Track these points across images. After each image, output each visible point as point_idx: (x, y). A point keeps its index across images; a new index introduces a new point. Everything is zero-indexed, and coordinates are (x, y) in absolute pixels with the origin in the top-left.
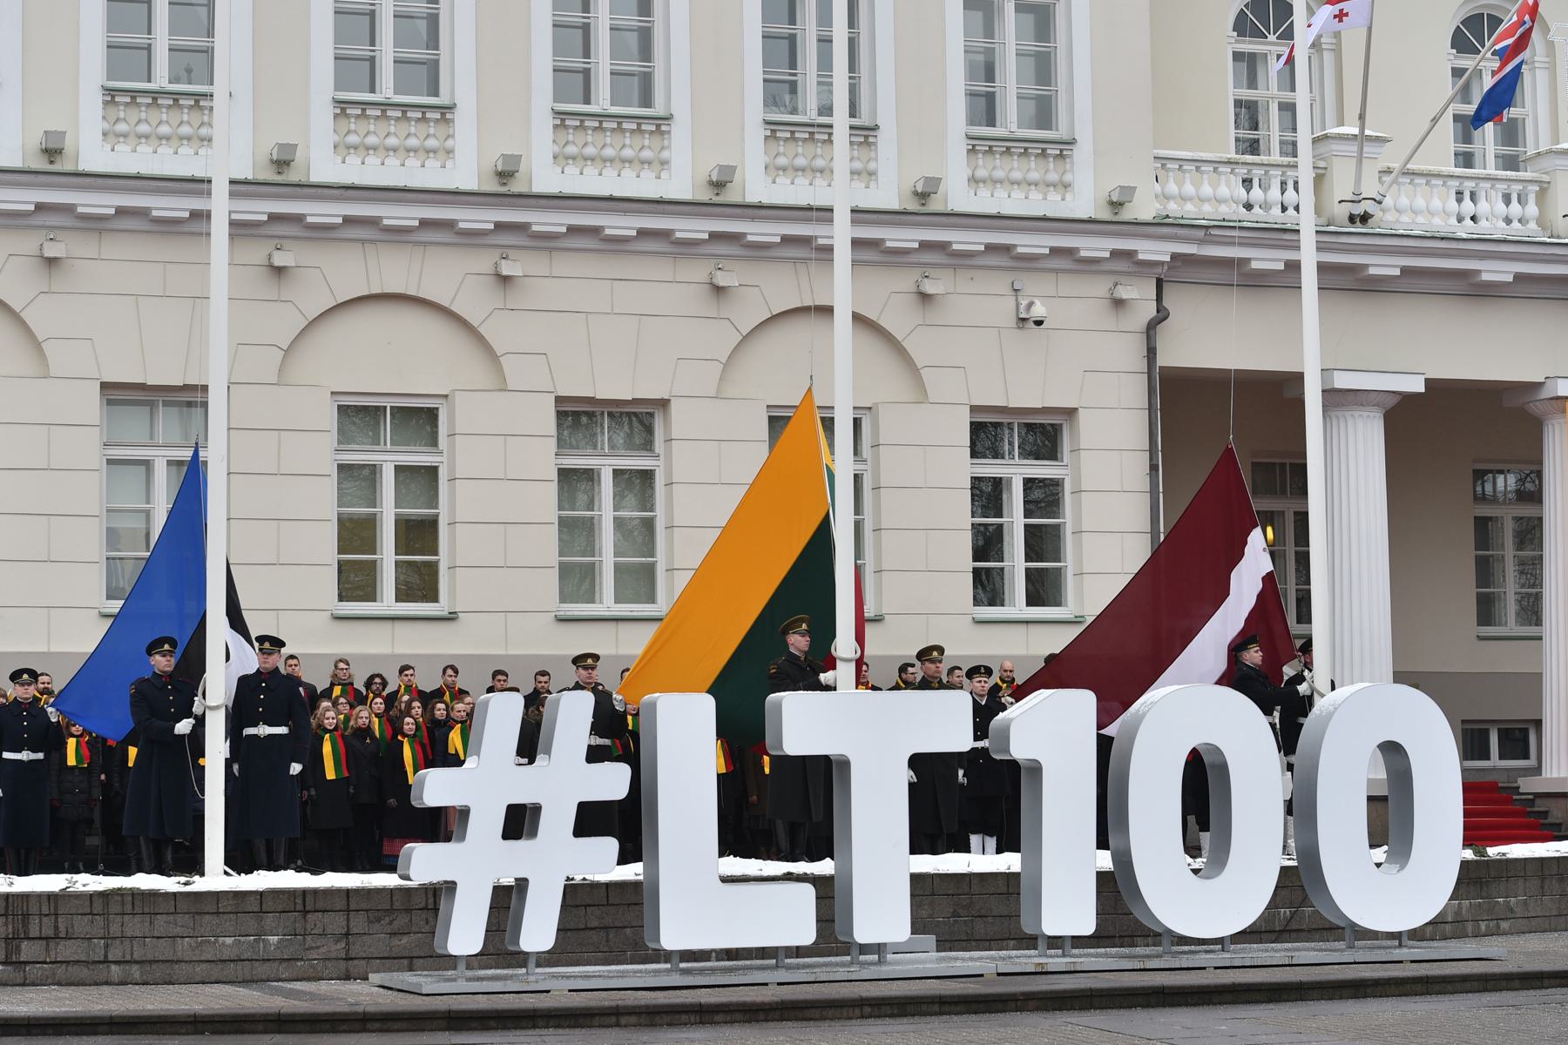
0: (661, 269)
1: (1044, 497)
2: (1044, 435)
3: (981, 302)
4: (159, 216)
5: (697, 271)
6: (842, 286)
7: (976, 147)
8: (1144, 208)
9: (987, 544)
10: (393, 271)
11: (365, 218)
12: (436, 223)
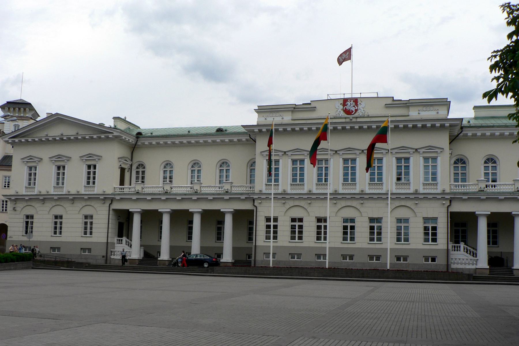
0: (382, 201)
1: (434, 229)
4: (321, 198)
7: (424, 184)
8: (448, 191)
11: (344, 197)
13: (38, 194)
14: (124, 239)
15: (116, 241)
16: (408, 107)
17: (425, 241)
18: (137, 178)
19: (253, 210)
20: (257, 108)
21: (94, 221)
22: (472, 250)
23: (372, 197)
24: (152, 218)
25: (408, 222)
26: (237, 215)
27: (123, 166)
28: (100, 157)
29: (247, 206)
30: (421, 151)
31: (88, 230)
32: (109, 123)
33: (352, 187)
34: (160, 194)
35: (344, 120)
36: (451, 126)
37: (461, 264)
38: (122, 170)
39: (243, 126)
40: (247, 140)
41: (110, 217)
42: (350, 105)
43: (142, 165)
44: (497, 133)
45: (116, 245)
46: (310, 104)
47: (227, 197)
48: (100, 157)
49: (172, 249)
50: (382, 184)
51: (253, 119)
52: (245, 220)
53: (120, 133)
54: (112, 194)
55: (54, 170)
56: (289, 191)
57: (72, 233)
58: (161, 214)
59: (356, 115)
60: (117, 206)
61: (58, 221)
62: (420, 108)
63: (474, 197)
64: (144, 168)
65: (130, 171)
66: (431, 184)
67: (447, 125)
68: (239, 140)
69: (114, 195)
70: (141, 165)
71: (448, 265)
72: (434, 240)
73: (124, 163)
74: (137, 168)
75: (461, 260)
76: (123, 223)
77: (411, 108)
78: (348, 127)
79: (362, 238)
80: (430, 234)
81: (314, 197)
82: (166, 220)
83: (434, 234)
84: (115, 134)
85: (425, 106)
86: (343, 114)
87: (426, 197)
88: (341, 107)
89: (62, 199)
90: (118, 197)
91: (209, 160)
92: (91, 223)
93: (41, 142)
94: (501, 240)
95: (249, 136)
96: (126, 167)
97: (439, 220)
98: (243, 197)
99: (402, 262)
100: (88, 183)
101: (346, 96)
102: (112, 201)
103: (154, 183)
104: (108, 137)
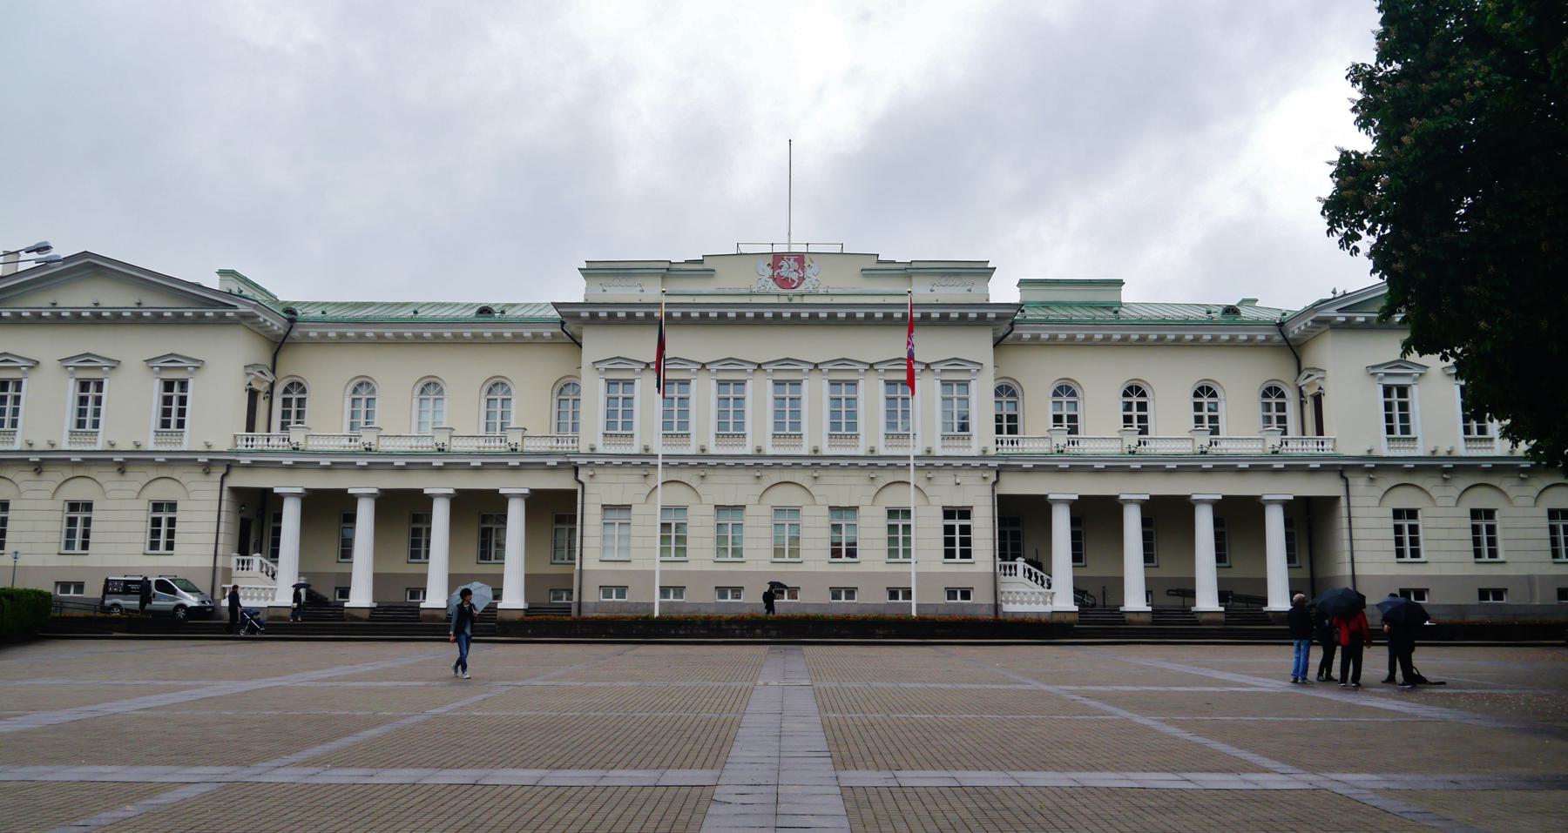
0: (857, 473)
1: (966, 530)
2: (965, 513)
3: (945, 480)
5: (866, 473)
6: (912, 477)
7: (944, 437)
9: (949, 542)
10: (787, 476)
11: (778, 462)
12: (796, 463)
13: (26, 448)
14: (256, 559)
15: (234, 565)
16: (909, 276)
17: (947, 556)
18: (286, 414)
19: (575, 492)
20: (584, 266)
21: (179, 516)
22: (1040, 573)
23: (837, 464)
24: (330, 511)
25: (968, 517)
26: (538, 503)
27: (255, 386)
28: (199, 365)
29: (562, 482)
30: (938, 368)
31: (163, 539)
32: (214, 282)
33: (792, 441)
34: (354, 454)
35: (774, 300)
36: (999, 318)
37: (1022, 602)
38: (253, 395)
39: (556, 305)
40: (553, 335)
41: (224, 507)
42: (786, 265)
43: (300, 384)
44: (1080, 336)
45: (235, 573)
46: (701, 262)
47: (514, 462)
48: (199, 365)
49: (379, 580)
50: (857, 436)
51: (575, 291)
52: (555, 512)
53: (255, 307)
54: (229, 452)
55: (71, 391)
56: (713, 450)
57: (120, 550)
58: (352, 500)
59: (801, 289)
60: (240, 480)
61: (80, 516)
62: (936, 280)
63: (1044, 467)
64: (304, 391)
65: (274, 398)
66: (1476, 440)
67: (991, 315)
68: (534, 335)
69: (238, 453)
70: (297, 386)
71: (996, 606)
72: (966, 554)
73: (257, 379)
74: (286, 391)
75: (1024, 597)
76: (255, 520)
77: (915, 280)
78: (787, 314)
79: (873, 557)
80: (957, 542)
81: (826, 462)
82: (365, 514)
83: (966, 542)
84: (243, 309)
85: (943, 275)
86: (772, 287)
87: (949, 465)
88: (769, 271)
89: (92, 461)
90: (245, 460)
91: (464, 377)
92: (172, 522)
93: (37, 320)
94: (1089, 552)
95: (570, 327)
96: (262, 388)
97: (974, 514)
98: (552, 462)
99: (900, 600)
100: (165, 424)
101: (777, 249)
102: (229, 467)
103: (326, 427)
104: (222, 316)
